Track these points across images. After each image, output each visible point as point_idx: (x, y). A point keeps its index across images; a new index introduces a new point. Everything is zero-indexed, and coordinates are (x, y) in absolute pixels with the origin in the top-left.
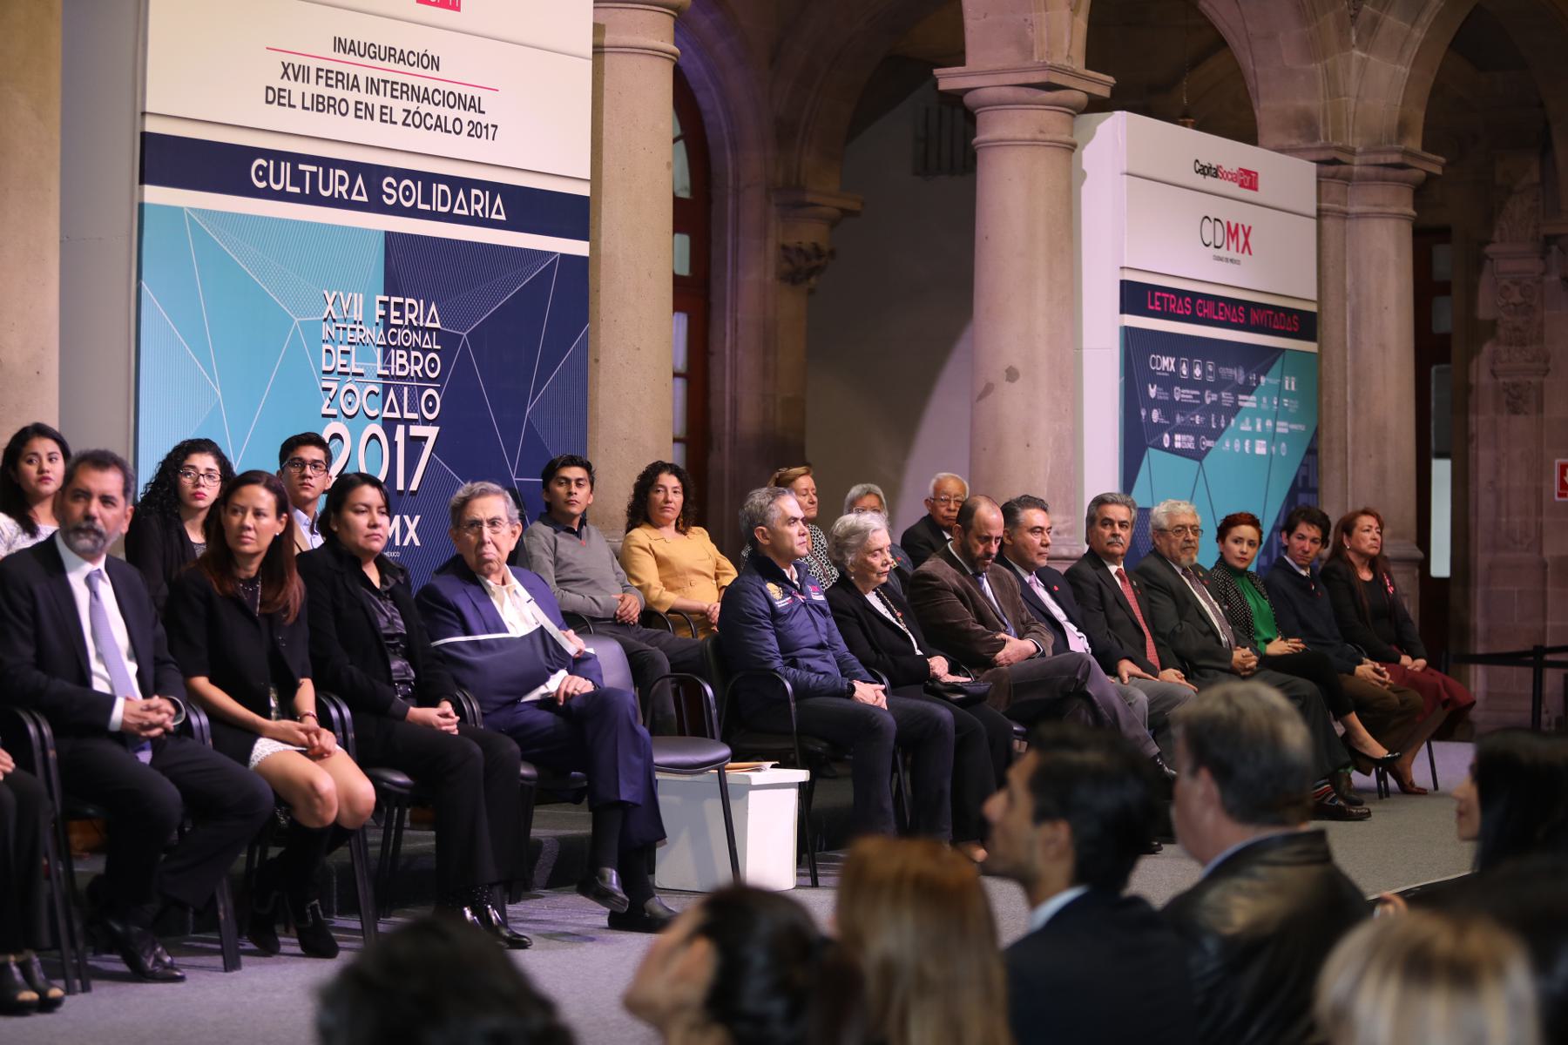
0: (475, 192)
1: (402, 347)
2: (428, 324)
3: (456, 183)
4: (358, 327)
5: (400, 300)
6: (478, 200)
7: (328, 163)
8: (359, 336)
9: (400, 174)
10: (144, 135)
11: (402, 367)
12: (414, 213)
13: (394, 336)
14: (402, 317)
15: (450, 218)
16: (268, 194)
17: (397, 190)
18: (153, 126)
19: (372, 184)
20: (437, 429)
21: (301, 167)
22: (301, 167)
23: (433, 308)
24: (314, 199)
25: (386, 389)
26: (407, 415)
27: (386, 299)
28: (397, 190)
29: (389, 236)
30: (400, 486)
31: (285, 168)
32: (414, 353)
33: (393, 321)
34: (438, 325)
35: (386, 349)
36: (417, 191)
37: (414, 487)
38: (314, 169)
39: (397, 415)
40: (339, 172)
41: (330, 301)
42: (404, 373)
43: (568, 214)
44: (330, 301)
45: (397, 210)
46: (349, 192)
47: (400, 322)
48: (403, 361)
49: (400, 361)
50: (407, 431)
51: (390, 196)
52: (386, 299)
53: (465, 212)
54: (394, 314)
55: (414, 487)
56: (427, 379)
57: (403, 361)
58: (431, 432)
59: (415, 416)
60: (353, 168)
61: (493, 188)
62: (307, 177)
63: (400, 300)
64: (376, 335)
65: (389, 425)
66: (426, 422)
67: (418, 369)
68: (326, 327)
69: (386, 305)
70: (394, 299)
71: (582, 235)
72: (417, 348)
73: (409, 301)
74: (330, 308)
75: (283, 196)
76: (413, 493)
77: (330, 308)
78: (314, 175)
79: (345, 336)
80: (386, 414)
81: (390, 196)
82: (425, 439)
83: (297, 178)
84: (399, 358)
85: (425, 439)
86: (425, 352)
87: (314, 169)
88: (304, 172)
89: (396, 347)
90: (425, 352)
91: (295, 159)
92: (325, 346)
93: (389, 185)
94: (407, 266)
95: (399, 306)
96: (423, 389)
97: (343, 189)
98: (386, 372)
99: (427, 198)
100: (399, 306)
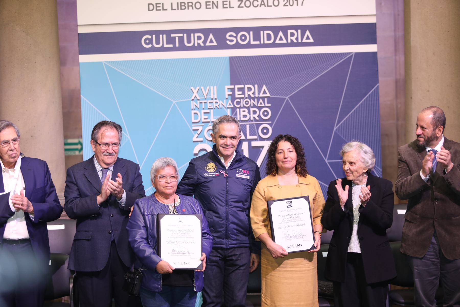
0: (289, 32)
1: (244, 107)
2: (261, 95)
3: (276, 30)
4: (214, 101)
5: (242, 86)
6: (292, 35)
7: (189, 32)
8: (214, 105)
9: (237, 30)
11: (245, 116)
12: (249, 46)
13: (238, 103)
14: (244, 93)
15: (274, 45)
16: (153, 50)
17: (236, 37)
18: (81, 30)
19: (220, 37)
21: (172, 35)
22: (172, 35)
23: (264, 88)
24: (182, 48)
26: (249, 137)
27: (232, 87)
28: (236, 37)
29: (232, 59)
31: (163, 38)
32: (252, 110)
33: (237, 96)
34: (268, 95)
36: (250, 37)
38: (181, 35)
40: (196, 35)
41: (195, 91)
43: (366, 33)
44: (195, 91)
45: (237, 46)
46: (205, 42)
47: (243, 96)
48: (246, 113)
49: (242, 113)
51: (232, 41)
52: (232, 87)
53: (284, 41)
54: (237, 92)
57: (246, 113)
59: (255, 137)
60: (206, 32)
61: (303, 28)
62: (176, 39)
63: (242, 86)
67: (256, 116)
68: (193, 104)
69: (233, 90)
70: (237, 87)
71: (373, 41)
72: (254, 106)
73: (247, 86)
74: (195, 94)
75: (163, 49)
77: (195, 94)
78: (181, 39)
81: (232, 41)
82: (263, 147)
83: (170, 40)
85: (263, 147)
86: (260, 108)
87: (181, 35)
88: (175, 37)
89: (240, 108)
90: (260, 108)
91: (168, 33)
92: (193, 112)
93: (231, 36)
94: (240, 71)
95: (239, 89)
96: (258, 126)
97: (201, 42)
99: (257, 37)
100: (239, 89)
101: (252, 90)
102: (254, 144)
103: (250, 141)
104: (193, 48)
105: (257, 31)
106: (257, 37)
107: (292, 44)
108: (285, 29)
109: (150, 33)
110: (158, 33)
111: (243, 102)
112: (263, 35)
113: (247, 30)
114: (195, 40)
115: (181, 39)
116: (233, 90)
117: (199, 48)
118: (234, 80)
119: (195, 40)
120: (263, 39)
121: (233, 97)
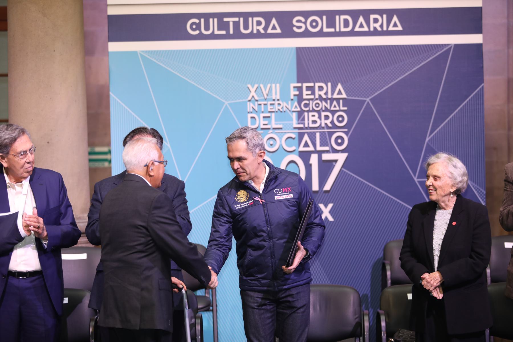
0: (372, 17)
1: (314, 110)
2: (335, 96)
3: (355, 14)
4: (276, 103)
5: (311, 84)
6: (376, 21)
7: (246, 15)
8: (277, 107)
9: (306, 14)
10: (109, 16)
11: (314, 122)
12: (321, 34)
14: (313, 93)
15: (352, 33)
16: (201, 37)
17: (305, 23)
18: (111, 11)
20: (345, 155)
21: (226, 20)
22: (226, 20)
23: (340, 87)
24: (238, 35)
25: (301, 136)
26: (319, 148)
27: (299, 85)
28: (305, 23)
29: (299, 51)
30: (315, 187)
31: (214, 23)
32: (323, 114)
33: (305, 97)
34: (344, 96)
35: (300, 114)
36: (322, 23)
37: (327, 187)
38: (236, 19)
39: (311, 148)
40: (256, 19)
41: (253, 90)
42: (317, 125)
43: (468, 19)
44: (253, 90)
45: (307, 34)
46: (266, 28)
47: (312, 97)
48: (316, 118)
49: (311, 119)
50: (320, 157)
51: (300, 27)
52: (299, 85)
53: (366, 29)
54: (305, 92)
55: (327, 187)
56: (335, 126)
57: (316, 118)
58: (341, 158)
59: (327, 148)
60: (268, 16)
61: (390, 13)
62: (230, 25)
63: (311, 84)
64: (295, 106)
65: (305, 156)
66: (335, 151)
67: (328, 122)
68: (250, 106)
69: (300, 89)
70: (305, 85)
72: (326, 110)
73: (317, 85)
74: (253, 93)
75: (213, 37)
76: (326, 192)
77: (253, 93)
78: (236, 25)
79: (266, 109)
80: (302, 149)
81: (300, 27)
82: (336, 161)
83: (223, 26)
84: (310, 119)
85: (336, 161)
86: (333, 112)
87: (236, 19)
88: (228, 22)
89: (308, 111)
90: (333, 112)
91: (220, 16)
92: (250, 115)
94: (310, 66)
95: (308, 88)
96: (331, 134)
97: (261, 28)
98: (301, 126)
99: (331, 23)
100: (308, 88)
101: (323, 89)
102: (325, 157)
103: (320, 153)
104: (251, 36)
105: (331, 16)
106: (331, 23)
107: (375, 33)
108: (366, 13)
109: (198, 16)
110: (207, 16)
111: (312, 105)
112: (339, 20)
113: (320, 14)
114: (254, 26)
115: (236, 25)
116: (300, 89)
117: (258, 35)
118: (302, 77)
119: (254, 26)
120: (340, 26)
121: (300, 98)
